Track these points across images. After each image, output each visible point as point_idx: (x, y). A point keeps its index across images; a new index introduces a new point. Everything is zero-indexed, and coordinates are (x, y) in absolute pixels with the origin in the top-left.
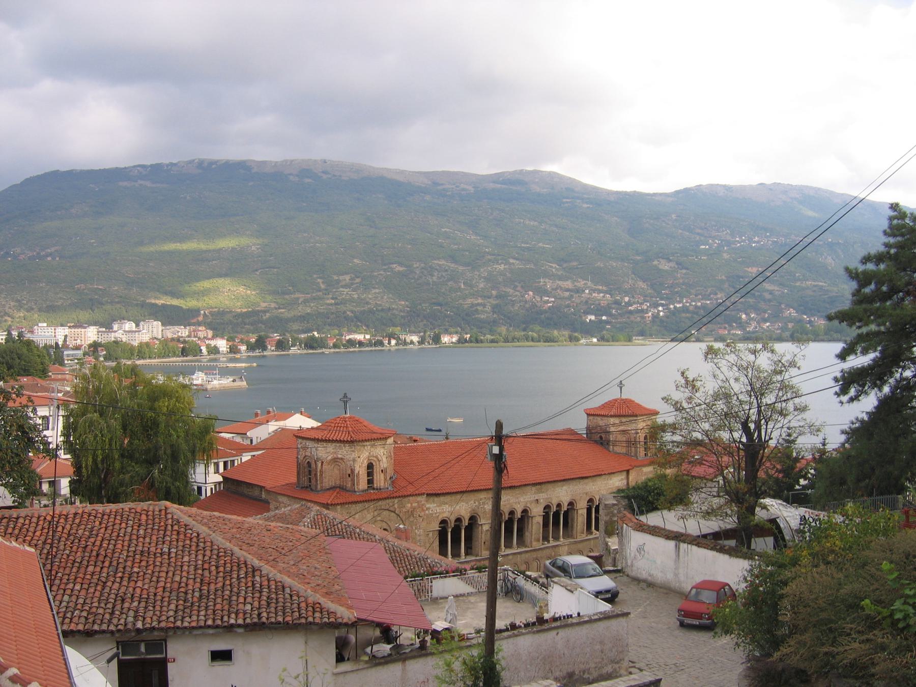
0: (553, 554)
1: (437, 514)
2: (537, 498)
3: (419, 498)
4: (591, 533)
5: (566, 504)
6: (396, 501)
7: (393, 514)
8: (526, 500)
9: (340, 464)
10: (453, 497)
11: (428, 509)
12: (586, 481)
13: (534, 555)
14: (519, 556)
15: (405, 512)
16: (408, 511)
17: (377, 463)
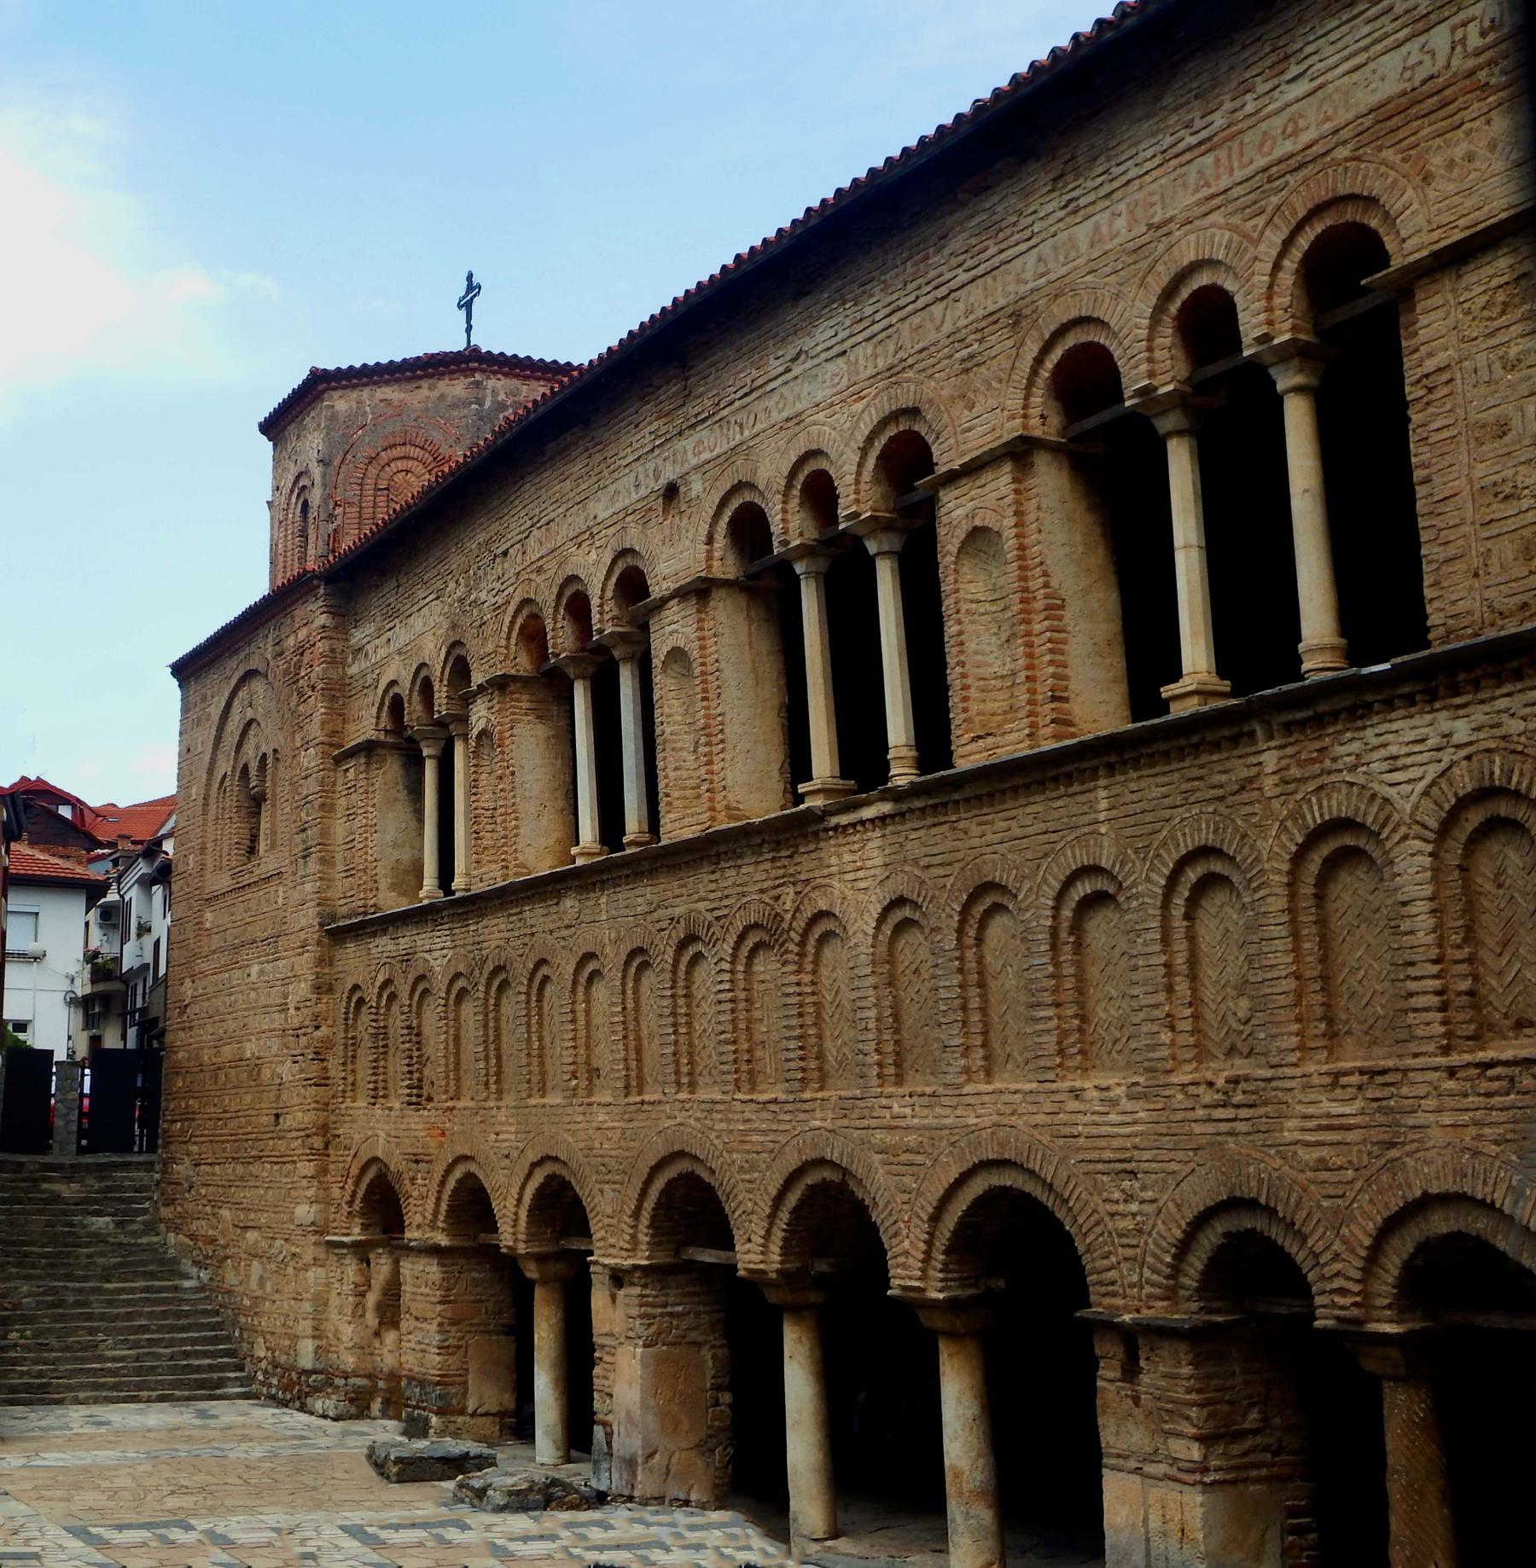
2: (670, 473)
8: (619, 505)
14: (604, 900)
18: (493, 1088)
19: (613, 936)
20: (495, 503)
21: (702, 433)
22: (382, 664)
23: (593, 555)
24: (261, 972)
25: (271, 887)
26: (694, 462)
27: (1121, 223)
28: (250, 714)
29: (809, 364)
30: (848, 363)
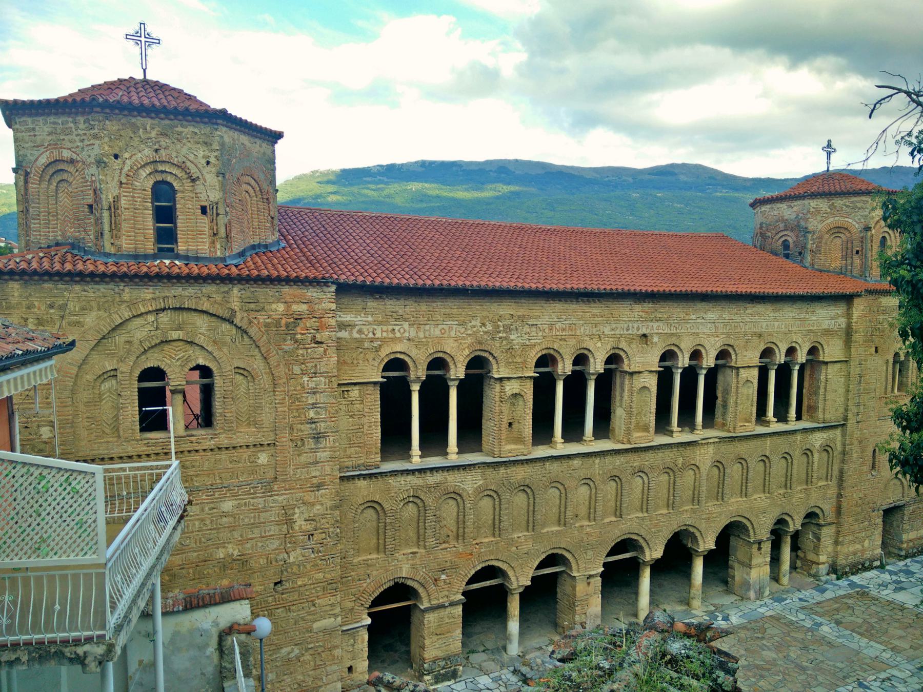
0: (680, 461)
1: (376, 344)
2: (644, 331)
3: (311, 293)
4: (767, 423)
5: (713, 354)
6: (236, 291)
7: (225, 327)
8: (617, 332)
9: (70, 179)
10: (423, 307)
11: (342, 326)
12: (760, 308)
13: (636, 461)
14: (597, 461)
15: (267, 325)
16: (278, 324)
17: (188, 184)
18: (510, 530)
19: (601, 472)
20: (523, 301)
21: (660, 324)
22: (384, 341)
23: (599, 345)
24: (238, 506)
25: (245, 454)
26: (656, 331)
27: (783, 326)
28: (175, 335)
29: (703, 321)
30: (715, 326)
